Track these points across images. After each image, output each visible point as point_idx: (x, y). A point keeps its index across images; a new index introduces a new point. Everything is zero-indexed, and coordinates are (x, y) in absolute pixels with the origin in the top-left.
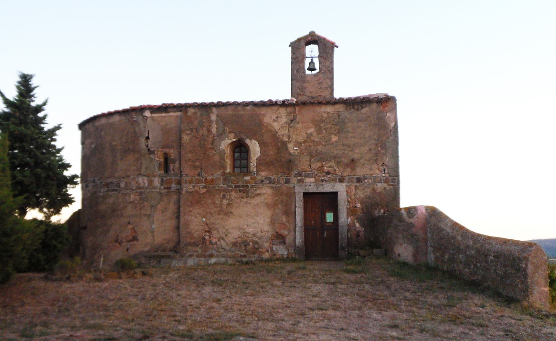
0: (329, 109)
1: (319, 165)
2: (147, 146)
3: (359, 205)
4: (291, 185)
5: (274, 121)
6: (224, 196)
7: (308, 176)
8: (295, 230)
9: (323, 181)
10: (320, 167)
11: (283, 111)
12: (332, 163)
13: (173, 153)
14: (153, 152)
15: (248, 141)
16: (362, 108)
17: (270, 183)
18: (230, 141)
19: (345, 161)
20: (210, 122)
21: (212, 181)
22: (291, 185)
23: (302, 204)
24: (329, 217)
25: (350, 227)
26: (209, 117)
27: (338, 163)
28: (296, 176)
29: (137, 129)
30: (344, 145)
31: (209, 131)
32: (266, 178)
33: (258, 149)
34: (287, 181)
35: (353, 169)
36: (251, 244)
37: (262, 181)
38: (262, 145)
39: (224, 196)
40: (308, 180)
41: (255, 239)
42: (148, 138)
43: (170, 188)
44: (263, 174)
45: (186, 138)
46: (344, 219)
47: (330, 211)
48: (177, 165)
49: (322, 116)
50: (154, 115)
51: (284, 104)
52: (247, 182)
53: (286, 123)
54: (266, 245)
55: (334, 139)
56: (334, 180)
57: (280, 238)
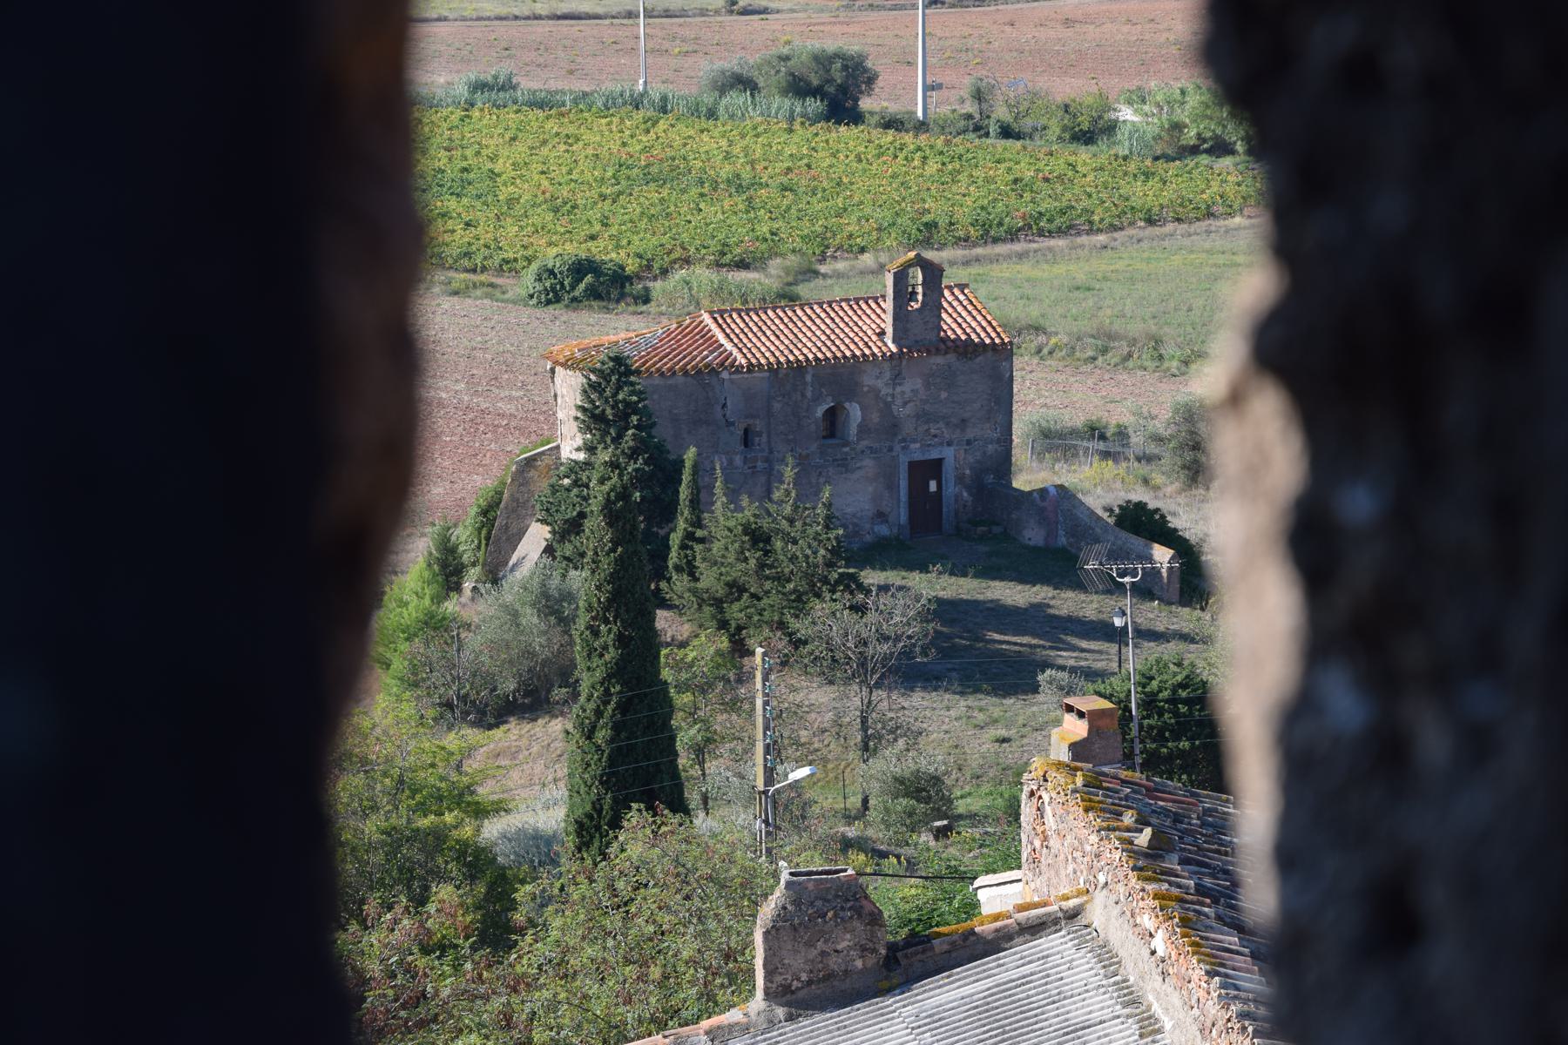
0: (939, 360)
1: (926, 427)
2: (724, 416)
3: (968, 472)
4: (894, 454)
5: (877, 378)
6: (820, 473)
7: (914, 441)
8: (899, 507)
10: (927, 430)
12: (941, 425)
13: (759, 425)
14: (733, 424)
15: (847, 405)
16: (976, 356)
18: (827, 407)
19: (954, 420)
20: (805, 383)
21: (808, 455)
23: (906, 475)
24: (933, 486)
25: (957, 497)
26: (804, 378)
27: (947, 424)
28: (900, 441)
29: (710, 394)
30: (953, 402)
31: (803, 395)
33: (859, 413)
34: (891, 449)
35: (963, 430)
36: (851, 527)
37: (863, 452)
39: (820, 473)
41: (855, 520)
42: (724, 406)
43: (755, 467)
44: (865, 443)
45: (777, 406)
46: (951, 489)
47: (933, 479)
48: (764, 438)
49: (931, 369)
50: (733, 376)
52: (846, 453)
53: (891, 379)
54: (868, 526)
55: (944, 395)
56: (941, 444)
57: (881, 516)
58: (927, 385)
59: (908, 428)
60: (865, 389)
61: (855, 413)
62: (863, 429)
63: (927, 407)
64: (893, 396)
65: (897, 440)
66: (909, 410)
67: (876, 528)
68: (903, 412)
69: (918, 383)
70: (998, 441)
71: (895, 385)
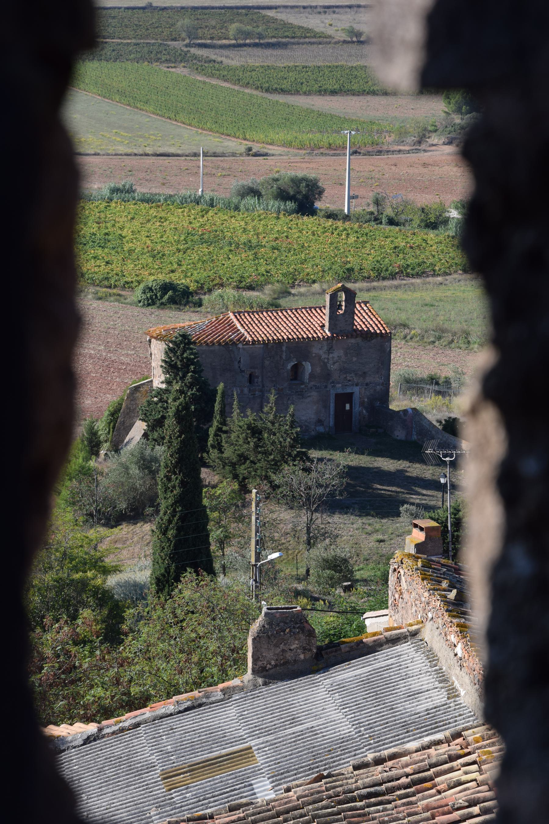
0: (353, 341)
1: (345, 376)
3: (366, 400)
4: (328, 389)
5: (320, 349)
7: (339, 383)
8: (329, 417)
12: (353, 375)
13: (257, 372)
14: (243, 371)
15: (304, 363)
20: (282, 351)
22: (328, 389)
24: (348, 407)
27: (356, 374)
31: (281, 357)
32: (314, 386)
33: (310, 367)
38: (312, 365)
40: (338, 386)
42: (239, 362)
44: (312, 383)
45: (267, 363)
46: (357, 409)
48: (260, 380)
54: (313, 427)
55: (355, 359)
56: (353, 385)
57: (320, 422)
58: (346, 354)
60: (314, 355)
61: (308, 367)
62: (312, 376)
64: (328, 359)
66: (336, 366)
67: (317, 428)
68: (333, 367)
69: (341, 353)
70: (382, 384)
71: (329, 353)
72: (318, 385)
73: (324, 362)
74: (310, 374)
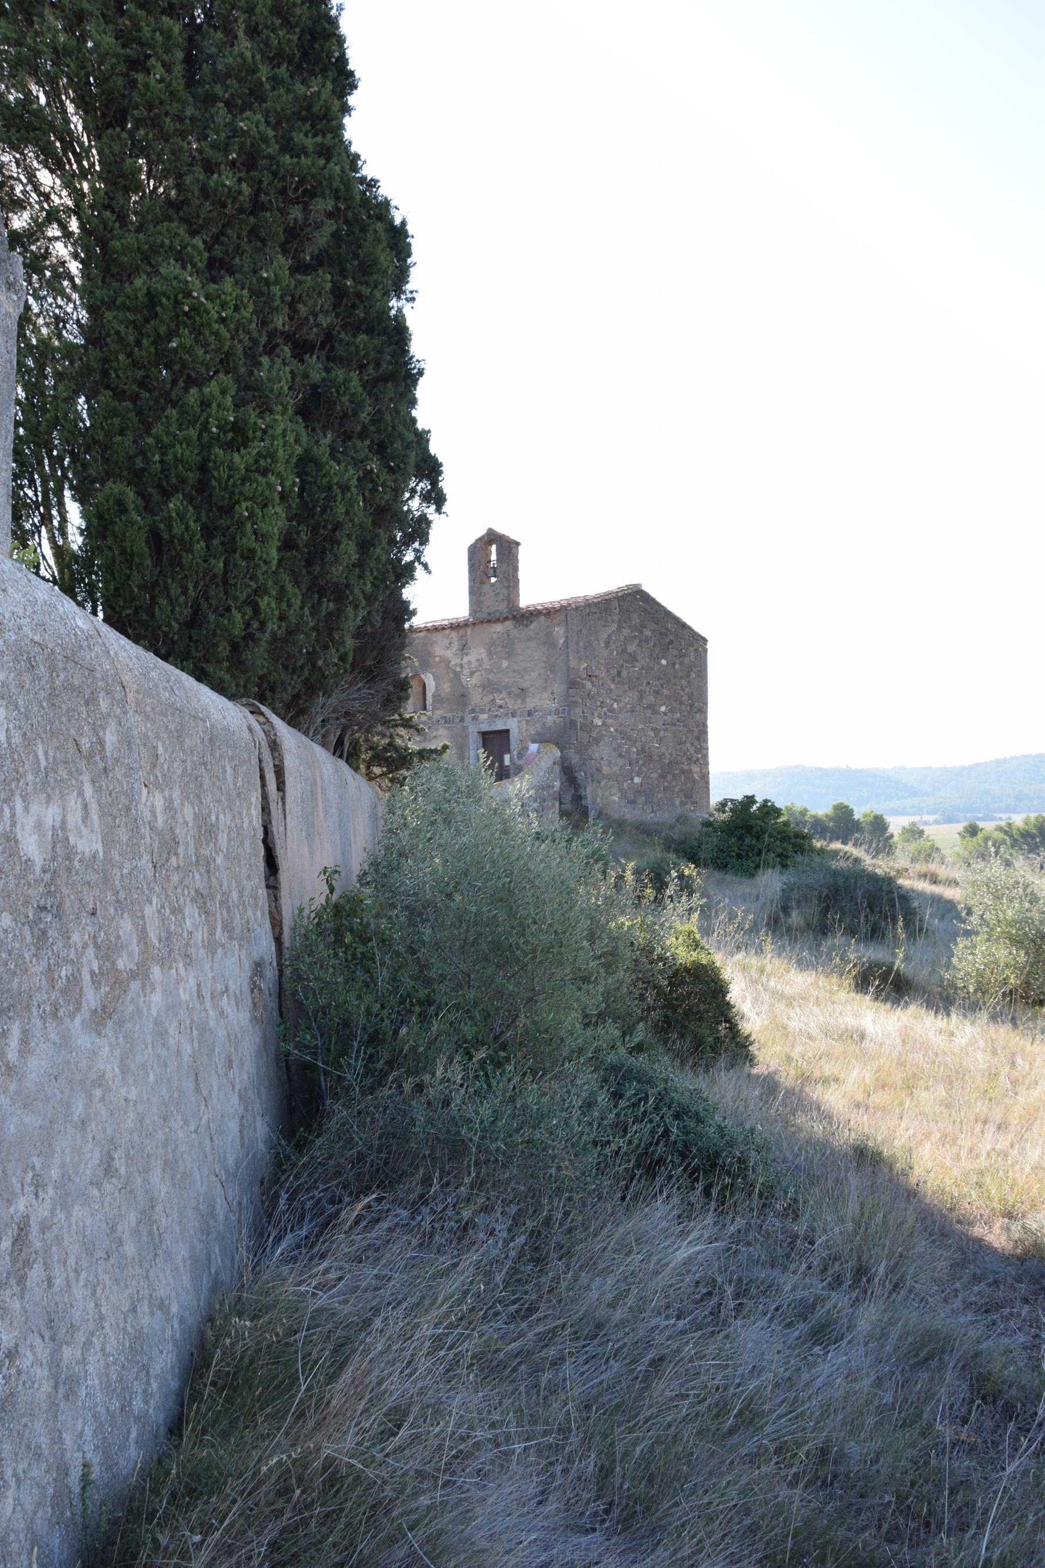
0: (498, 628)
4: (465, 724)
5: (448, 648)
7: (482, 712)
9: (496, 716)
11: (454, 635)
12: (504, 695)
17: (446, 722)
22: (465, 724)
27: (509, 694)
30: (514, 671)
33: (433, 683)
34: (462, 720)
35: (524, 700)
44: (439, 712)
51: (455, 626)
56: (507, 715)
58: (490, 654)
59: (476, 698)
60: (437, 659)
63: (491, 677)
65: (467, 710)
66: (475, 680)
68: (471, 682)
72: (449, 715)
73: (455, 672)
74: (434, 696)
